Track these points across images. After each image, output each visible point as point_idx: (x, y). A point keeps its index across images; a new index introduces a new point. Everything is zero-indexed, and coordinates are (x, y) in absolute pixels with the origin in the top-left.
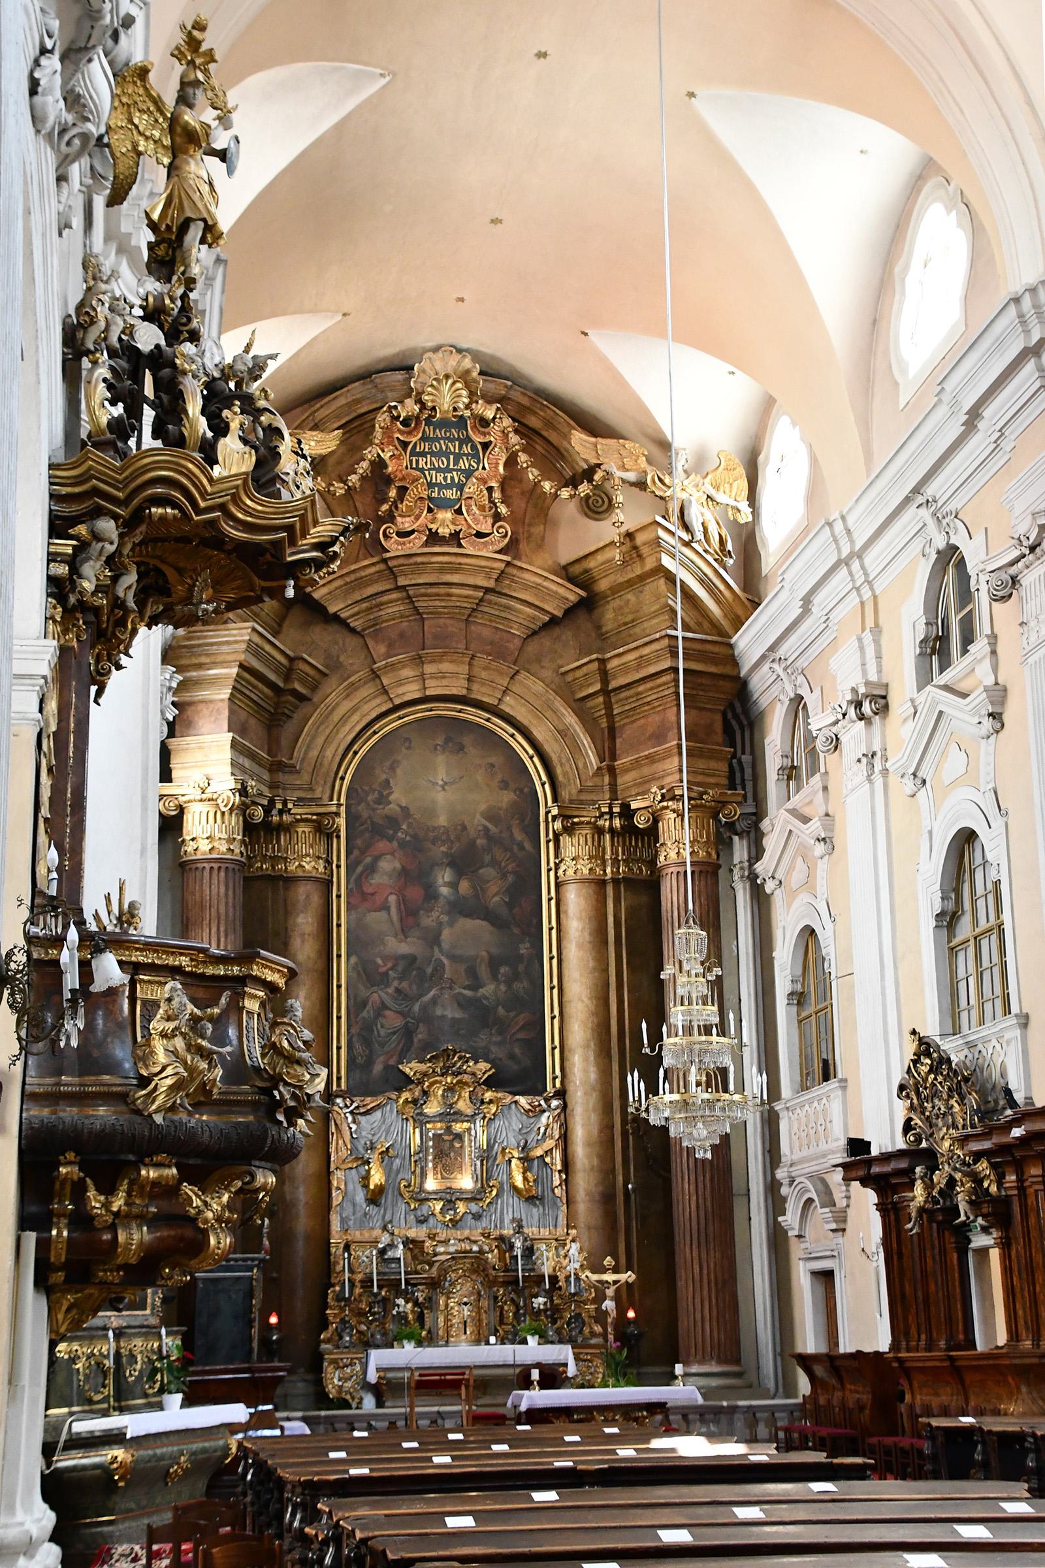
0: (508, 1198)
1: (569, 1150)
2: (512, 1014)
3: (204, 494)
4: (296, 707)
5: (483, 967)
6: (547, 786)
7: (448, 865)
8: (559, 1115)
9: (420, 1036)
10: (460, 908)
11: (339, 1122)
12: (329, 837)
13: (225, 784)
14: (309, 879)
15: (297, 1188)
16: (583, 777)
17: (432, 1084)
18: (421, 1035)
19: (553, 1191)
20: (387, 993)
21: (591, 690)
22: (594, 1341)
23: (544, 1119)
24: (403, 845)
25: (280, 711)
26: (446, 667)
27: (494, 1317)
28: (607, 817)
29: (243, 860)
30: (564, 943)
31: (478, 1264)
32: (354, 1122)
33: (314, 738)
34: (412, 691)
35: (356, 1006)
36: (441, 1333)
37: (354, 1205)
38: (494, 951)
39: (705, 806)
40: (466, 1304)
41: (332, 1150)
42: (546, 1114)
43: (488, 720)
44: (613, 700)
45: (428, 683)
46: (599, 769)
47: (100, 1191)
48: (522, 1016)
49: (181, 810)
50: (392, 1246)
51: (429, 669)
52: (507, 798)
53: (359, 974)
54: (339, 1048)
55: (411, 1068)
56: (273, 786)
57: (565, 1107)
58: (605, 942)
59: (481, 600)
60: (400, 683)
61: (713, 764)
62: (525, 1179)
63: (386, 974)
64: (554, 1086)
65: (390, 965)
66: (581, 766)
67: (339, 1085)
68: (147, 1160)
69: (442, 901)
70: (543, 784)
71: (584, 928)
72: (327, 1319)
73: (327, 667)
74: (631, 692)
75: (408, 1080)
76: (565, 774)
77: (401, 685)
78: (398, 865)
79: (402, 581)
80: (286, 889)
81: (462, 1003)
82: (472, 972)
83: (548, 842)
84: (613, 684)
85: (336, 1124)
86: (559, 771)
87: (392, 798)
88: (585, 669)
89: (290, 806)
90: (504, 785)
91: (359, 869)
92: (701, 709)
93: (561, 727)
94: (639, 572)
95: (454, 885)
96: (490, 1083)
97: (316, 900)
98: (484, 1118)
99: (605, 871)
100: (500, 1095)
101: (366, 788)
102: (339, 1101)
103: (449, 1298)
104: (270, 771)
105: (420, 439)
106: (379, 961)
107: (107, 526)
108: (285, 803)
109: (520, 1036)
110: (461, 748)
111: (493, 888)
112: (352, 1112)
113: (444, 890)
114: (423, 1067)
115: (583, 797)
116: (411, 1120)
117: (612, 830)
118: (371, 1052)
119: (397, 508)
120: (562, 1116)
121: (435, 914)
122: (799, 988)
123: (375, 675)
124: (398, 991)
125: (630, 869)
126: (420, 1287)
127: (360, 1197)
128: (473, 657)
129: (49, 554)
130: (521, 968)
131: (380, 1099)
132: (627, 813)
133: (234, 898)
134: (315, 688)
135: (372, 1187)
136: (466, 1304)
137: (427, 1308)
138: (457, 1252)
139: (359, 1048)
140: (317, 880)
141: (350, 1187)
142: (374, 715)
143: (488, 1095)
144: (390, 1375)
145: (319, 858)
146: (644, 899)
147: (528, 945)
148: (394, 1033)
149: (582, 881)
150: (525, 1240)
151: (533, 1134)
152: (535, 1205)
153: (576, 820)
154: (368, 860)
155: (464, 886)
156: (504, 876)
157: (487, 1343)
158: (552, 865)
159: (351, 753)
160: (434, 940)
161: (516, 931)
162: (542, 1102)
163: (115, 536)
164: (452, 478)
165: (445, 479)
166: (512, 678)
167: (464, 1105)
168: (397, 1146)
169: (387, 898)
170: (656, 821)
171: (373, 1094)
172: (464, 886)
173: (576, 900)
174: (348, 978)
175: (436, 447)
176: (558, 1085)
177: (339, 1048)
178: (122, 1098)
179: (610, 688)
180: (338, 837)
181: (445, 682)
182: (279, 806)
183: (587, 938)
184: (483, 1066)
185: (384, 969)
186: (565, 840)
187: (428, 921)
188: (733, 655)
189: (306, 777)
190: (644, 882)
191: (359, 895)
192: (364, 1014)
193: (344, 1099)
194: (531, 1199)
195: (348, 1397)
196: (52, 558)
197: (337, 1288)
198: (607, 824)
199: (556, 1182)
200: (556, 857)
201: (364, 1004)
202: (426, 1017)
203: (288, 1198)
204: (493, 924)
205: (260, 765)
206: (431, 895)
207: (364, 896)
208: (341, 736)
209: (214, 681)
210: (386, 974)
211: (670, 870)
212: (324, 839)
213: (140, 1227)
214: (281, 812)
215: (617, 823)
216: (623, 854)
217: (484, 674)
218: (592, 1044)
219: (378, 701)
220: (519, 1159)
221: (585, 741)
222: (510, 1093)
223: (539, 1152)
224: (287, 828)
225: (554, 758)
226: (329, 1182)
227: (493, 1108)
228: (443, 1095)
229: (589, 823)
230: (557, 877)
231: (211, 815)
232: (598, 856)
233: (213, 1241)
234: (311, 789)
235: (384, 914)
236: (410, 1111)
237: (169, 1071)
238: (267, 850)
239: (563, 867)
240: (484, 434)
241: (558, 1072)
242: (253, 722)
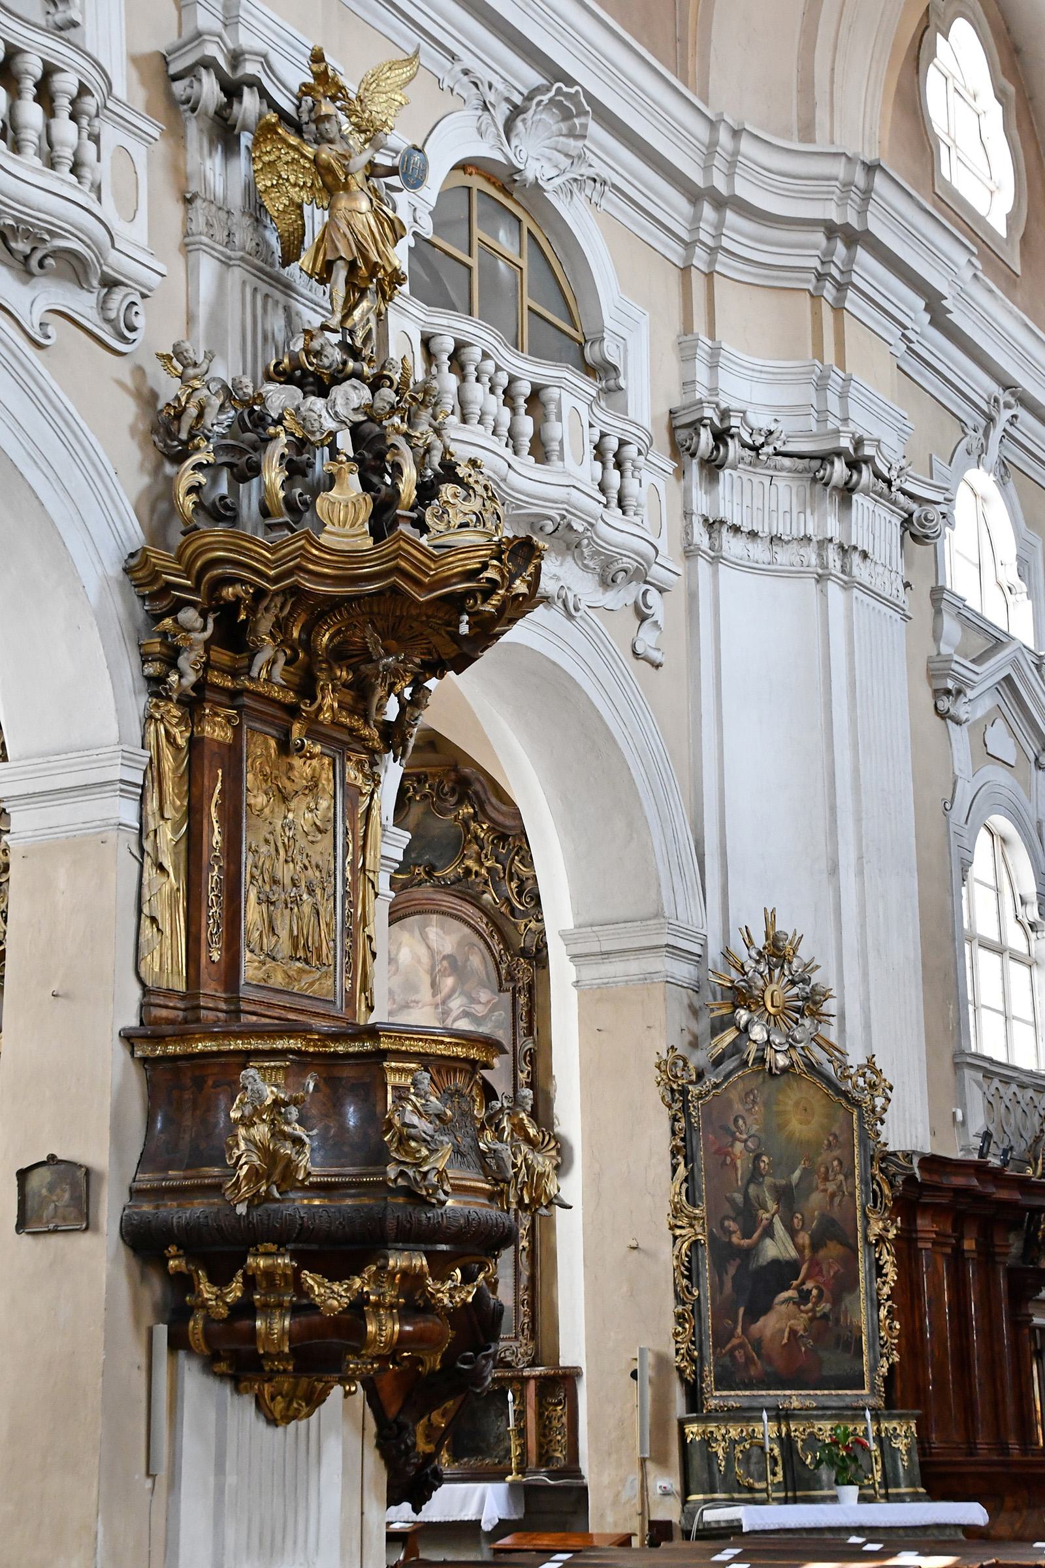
3: (267, 563)
47: (213, 1281)
68: (252, 1250)
107: (189, 616)
129: (142, 655)
163: (199, 623)
178: (217, 1188)
196: (145, 659)
213: (282, 1316)
233: (371, 1328)
237: (243, 1160)
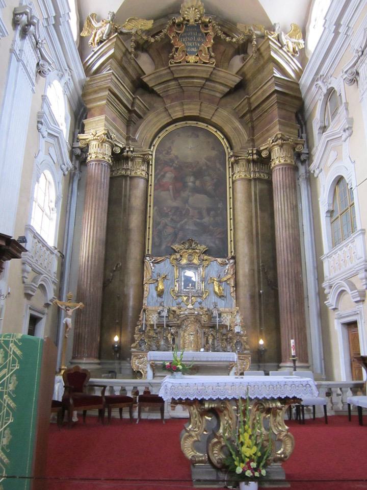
1: (237, 279)
2: (215, 228)
7: (192, 175)
8: (233, 265)
9: (180, 236)
10: (196, 190)
13: (101, 131)
18: (180, 235)
22: (245, 352)
23: (227, 268)
24: (175, 168)
26: (191, 106)
27: (203, 341)
30: (236, 203)
31: (197, 319)
32: (153, 266)
34: (179, 115)
35: (156, 224)
36: (181, 346)
37: (152, 297)
39: (289, 144)
40: (192, 335)
42: (228, 265)
45: (185, 111)
46: (248, 140)
49: (88, 145)
50: (163, 311)
51: (185, 107)
52: (214, 153)
54: (149, 239)
55: (176, 247)
57: (235, 263)
58: (251, 201)
59: (205, 84)
60: (175, 112)
61: (292, 130)
62: (219, 289)
63: (167, 213)
64: (231, 254)
72: (134, 339)
75: (175, 252)
79: (176, 76)
81: (196, 224)
82: (200, 213)
84: (253, 107)
86: (233, 141)
87: (172, 153)
88: (242, 104)
90: (213, 149)
92: (287, 111)
94: (262, 62)
95: (194, 183)
96: (205, 253)
100: (210, 258)
102: (147, 258)
103: (185, 332)
105: (184, 32)
106: (165, 208)
108: (129, 148)
109: (218, 236)
110: (198, 136)
112: (152, 262)
113: (190, 184)
114: (181, 247)
118: (161, 242)
119: (175, 54)
122: (331, 208)
123: (166, 110)
124: (172, 219)
125: (260, 175)
126: (174, 327)
127: (155, 294)
128: (202, 103)
132: (259, 153)
134: (145, 114)
136: (192, 335)
137: (176, 336)
139: (156, 239)
143: (206, 257)
144: (156, 362)
146: (265, 186)
147: (221, 204)
149: (242, 179)
151: (223, 273)
152: (223, 300)
153: (240, 158)
155: (198, 183)
160: (186, 201)
164: (195, 44)
165: (192, 44)
167: (196, 261)
172: (198, 183)
173: (240, 187)
174: (153, 214)
175: (189, 34)
176: (233, 254)
179: (252, 109)
181: (191, 111)
182: (127, 149)
184: (204, 246)
185: (166, 212)
188: (299, 88)
190: (266, 180)
191: (159, 185)
194: (221, 297)
195: (141, 371)
197: (140, 327)
198: (251, 157)
200: (232, 172)
201: (159, 223)
202: (182, 229)
204: (208, 196)
205: (121, 135)
206: (185, 186)
209: (101, 99)
210: (167, 213)
211: (276, 168)
214: (128, 152)
215: (255, 157)
217: (206, 109)
218: (246, 239)
219: (166, 119)
220: (217, 281)
223: (225, 279)
225: (232, 138)
226: (143, 289)
227: (207, 262)
229: (244, 159)
230: (232, 180)
231: (97, 145)
232: (248, 171)
235: (167, 192)
236: (174, 262)
239: (235, 176)
240: (206, 30)
241: (233, 250)
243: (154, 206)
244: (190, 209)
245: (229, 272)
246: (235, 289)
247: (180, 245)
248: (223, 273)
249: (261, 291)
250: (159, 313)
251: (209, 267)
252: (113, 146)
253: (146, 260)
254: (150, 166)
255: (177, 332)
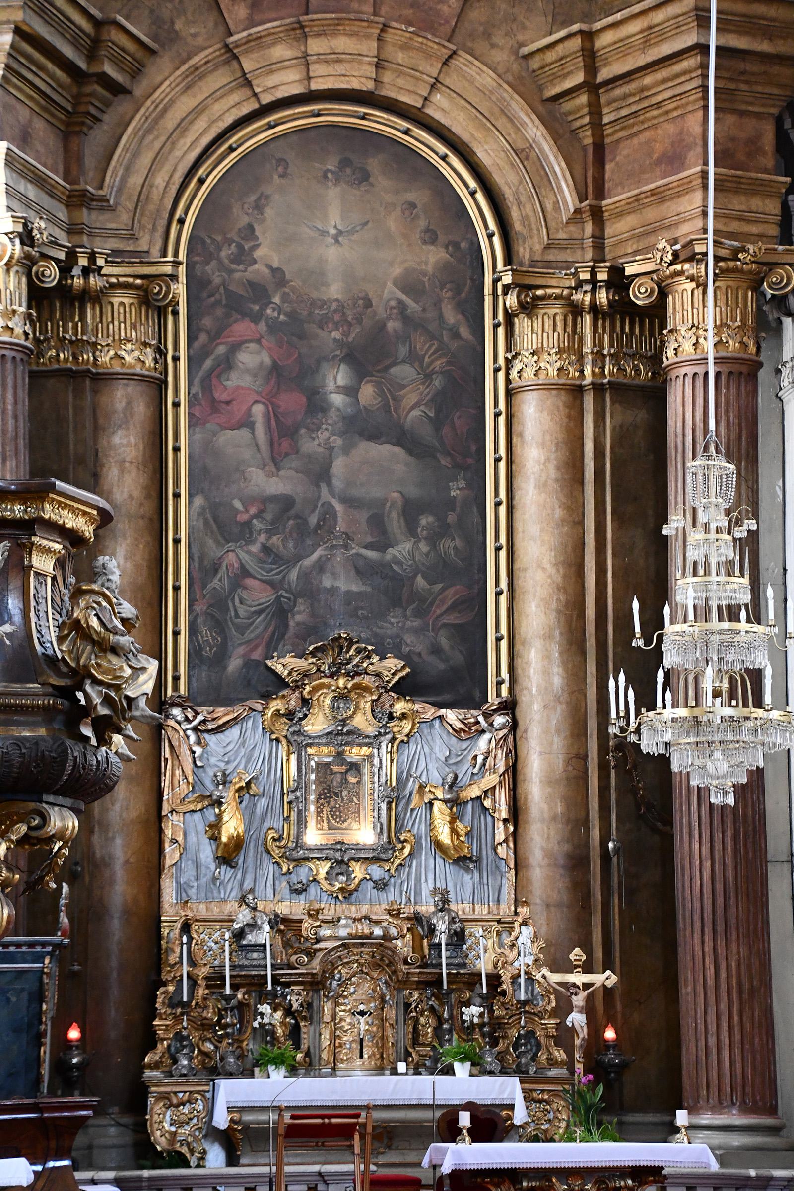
0: (427, 859)
1: (520, 790)
4: (108, 104)
5: (394, 515)
6: (496, 240)
7: (344, 359)
8: (505, 738)
9: (298, 618)
11: (175, 743)
12: (161, 312)
14: (130, 377)
15: (113, 838)
16: (552, 225)
17: (315, 689)
18: (300, 616)
19: (495, 849)
20: (249, 552)
21: (568, 84)
24: (274, 327)
25: (82, 108)
26: (342, 43)
28: (588, 287)
29: (28, 344)
30: (518, 482)
32: (199, 743)
33: (136, 155)
37: (197, 865)
38: (413, 492)
40: (362, 1013)
41: (166, 783)
42: (487, 736)
43: (407, 132)
44: (603, 100)
46: (577, 211)
48: (451, 591)
50: (253, 926)
51: (315, 46)
53: (206, 523)
54: (176, 634)
56: (73, 230)
57: (514, 726)
60: (270, 68)
62: (454, 831)
63: (248, 524)
65: (253, 510)
66: (549, 206)
67: (176, 688)
69: (333, 415)
70: (490, 236)
71: (548, 459)
73: (155, 38)
74: (633, 86)
75: (281, 683)
76: (524, 219)
77: (272, 72)
78: (267, 360)
80: (95, 392)
81: (363, 570)
82: (377, 523)
83: (496, 326)
84: (604, 74)
85: (171, 746)
86: (515, 214)
87: (258, 254)
88: (560, 49)
89: (100, 262)
90: (431, 237)
91: (208, 363)
92: (742, 113)
93: (520, 145)
95: (351, 391)
96: (403, 689)
97: (142, 409)
98: (393, 740)
99: (582, 372)
100: (417, 707)
101: (219, 238)
102: (176, 711)
103: (337, 1004)
104: (67, 206)
106: (238, 504)
108: (92, 257)
109: (446, 620)
110: (364, 177)
111: (411, 398)
112: (195, 729)
113: (337, 399)
114: (303, 664)
115: (551, 256)
116: (284, 741)
117: (594, 309)
118: (225, 639)
120: (511, 738)
121: (323, 435)
123: (231, 55)
124: (266, 549)
125: (621, 370)
126: (296, 988)
127: (207, 853)
128: (385, 27)
130: (451, 518)
131: (238, 710)
133: (16, 403)
134: (136, 73)
135: (224, 839)
136: (362, 1013)
138: (351, 936)
139: (206, 633)
140: (142, 379)
141: (192, 838)
142: (229, 120)
143: (400, 707)
145: (146, 345)
147: (462, 484)
148: (259, 613)
149: (547, 387)
150: (452, 921)
151: (467, 765)
152: (468, 870)
153: (540, 292)
154: (221, 350)
155: (367, 393)
156: (428, 377)
157: (394, 1072)
158: (501, 362)
159: (195, 180)
161: (444, 461)
162: (481, 719)
166: (445, 63)
168: (263, 779)
169: (249, 409)
170: (663, 294)
171: (228, 702)
172: (367, 393)
177: (176, 634)
180: (175, 313)
181: (340, 69)
182: (83, 262)
183: (553, 473)
184: (392, 663)
185: (244, 517)
186: (522, 324)
187: (311, 445)
189: (125, 217)
190: (642, 388)
192: (215, 583)
193: (184, 708)
194: (462, 861)
198: (588, 298)
199: (500, 836)
200: (508, 349)
203: (98, 855)
204: (410, 452)
207: (215, 406)
208: (178, 153)
210: (248, 524)
212: (153, 316)
214: (86, 272)
215: (603, 297)
216: (611, 346)
217: (400, 57)
219: (235, 97)
220: (445, 801)
221: (557, 166)
222: (433, 704)
223: (475, 792)
224: (97, 298)
225: (508, 194)
226: (161, 831)
228: (332, 707)
229: (558, 297)
230: (508, 381)
234: (133, 237)
235: (244, 433)
236: (283, 728)
238: (65, 331)
239: (517, 365)
241: (505, 675)
242: (39, 125)
243: (191, 496)
244: (338, 507)
245: (490, 760)
246: (511, 829)
247: (301, 655)
248: (467, 765)
249: (611, 845)
250: (239, 935)
251: (412, 740)
252: (27, 264)
253: (171, 722)
254: (170, 318)
255: (310, 1005)
